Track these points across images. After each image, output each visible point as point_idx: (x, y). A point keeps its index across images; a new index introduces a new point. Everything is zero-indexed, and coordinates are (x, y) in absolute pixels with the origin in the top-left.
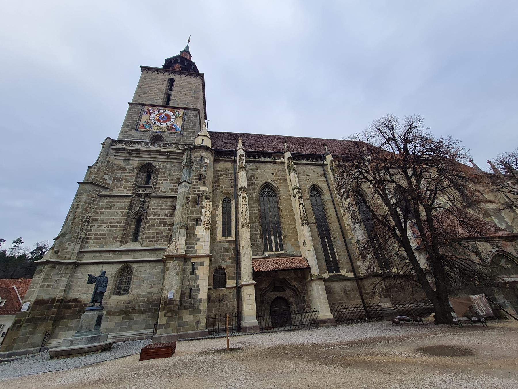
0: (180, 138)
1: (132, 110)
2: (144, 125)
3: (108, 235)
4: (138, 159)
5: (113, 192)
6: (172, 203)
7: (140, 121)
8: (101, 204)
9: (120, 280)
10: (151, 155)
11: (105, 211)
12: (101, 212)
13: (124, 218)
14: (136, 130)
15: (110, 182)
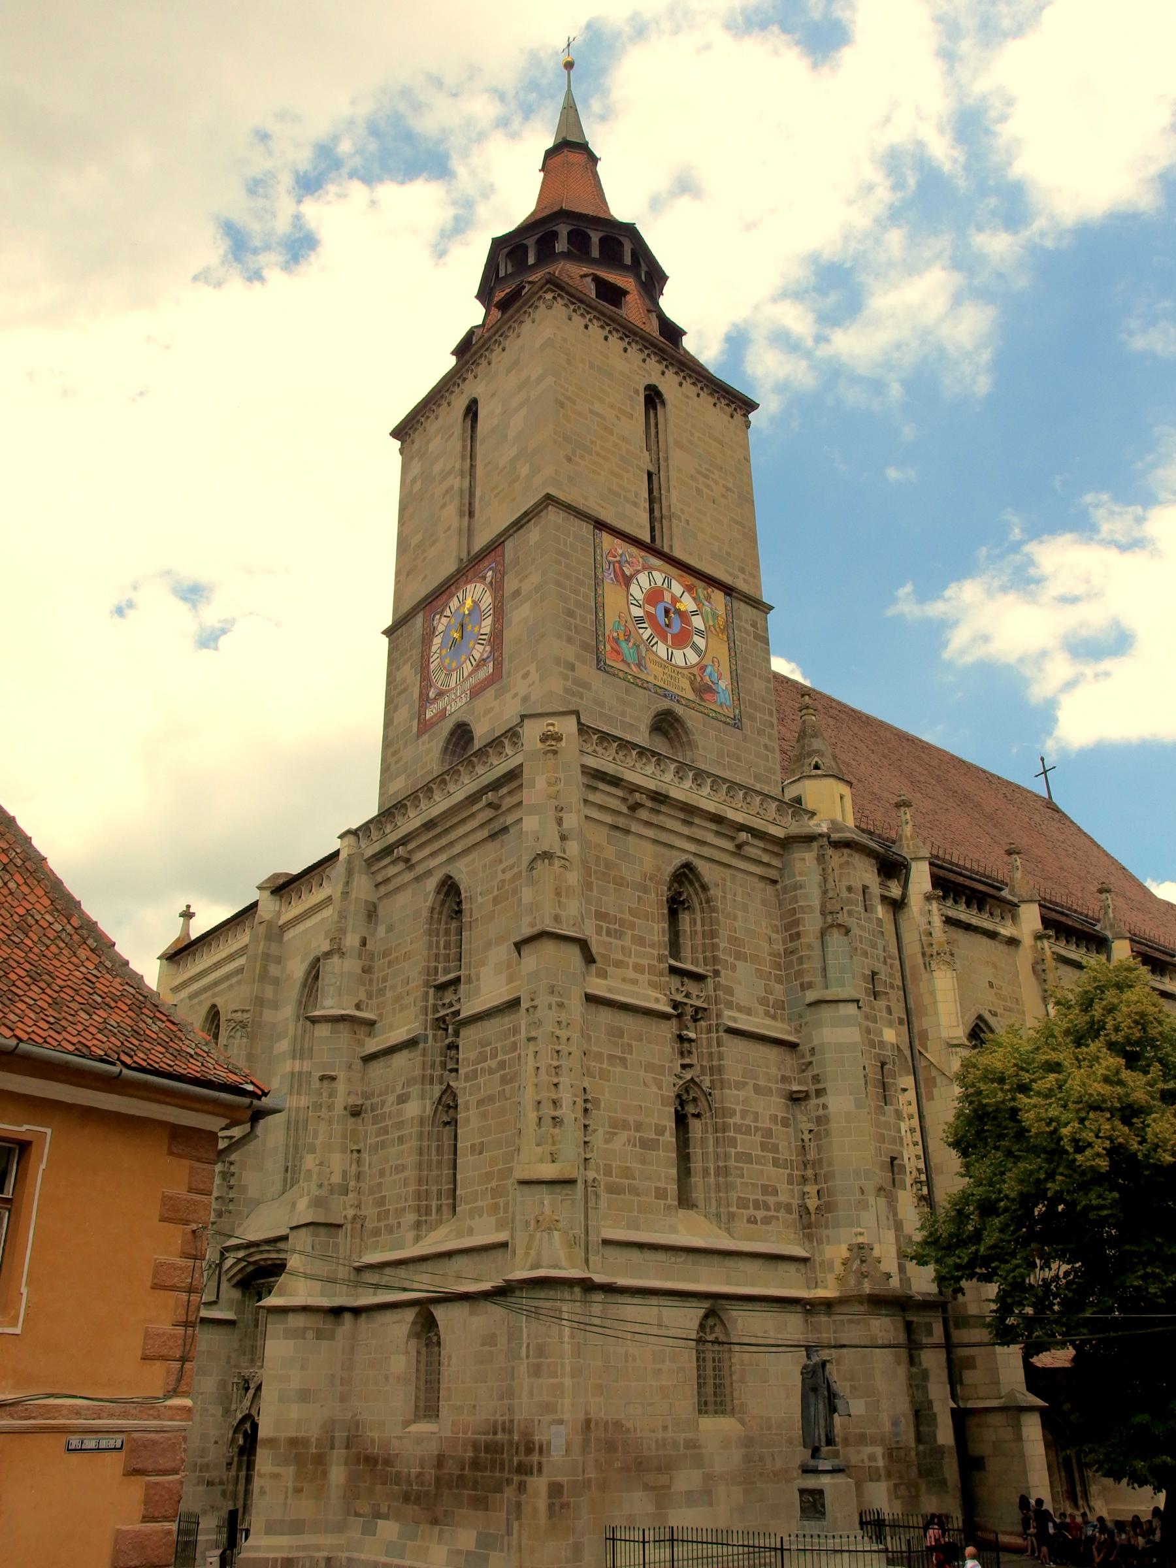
1: (565, 545)
4: (650, 833)
5: (609, 982)
6: (779, 1069)
10: (690, 824)
11: (612, 1069)
12: (604, 1075)
14: (601, 665)
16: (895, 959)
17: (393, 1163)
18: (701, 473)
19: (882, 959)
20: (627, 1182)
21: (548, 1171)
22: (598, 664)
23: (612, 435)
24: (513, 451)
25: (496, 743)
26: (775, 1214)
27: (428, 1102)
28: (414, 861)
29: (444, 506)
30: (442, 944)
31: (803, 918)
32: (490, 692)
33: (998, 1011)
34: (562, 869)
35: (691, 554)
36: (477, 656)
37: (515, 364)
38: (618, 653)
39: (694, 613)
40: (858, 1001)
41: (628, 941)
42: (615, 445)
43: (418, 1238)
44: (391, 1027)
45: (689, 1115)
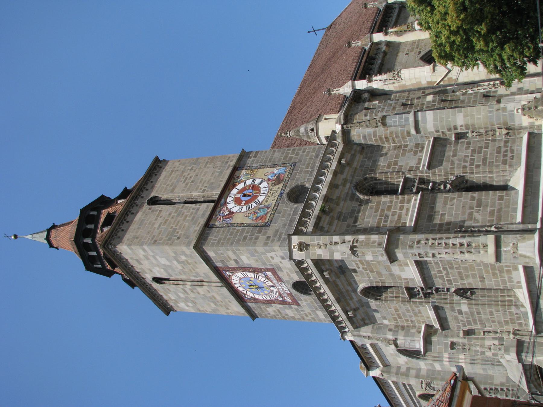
1: (215, 240)
2: (257, 218)
3: (495, 207)
8: (431, 228)
13: (465, 194)
16: (396, 95)
17: (489, 317)
18: (185, 181)
19: (396, 101)
20: (496, 213)
21: (491, 248)
22: (267, 226)
23: (168, 219)
24: (175, 262)
25: (304, 271)
26: (509, 147)
27: (462, 301)
28: (354, 307)
29: (198, 293)
30: (391, 295)
31: (379, 136)
32: (280, 273)
33: (418, 51)
34: (358, 242)
35: (220, 185)
36: (264, 279)
37: (138, 261)
39: (245, 184)
40: (415, 112)
41: (390, 213)
42: (173, 218)
43: (523, 306)
44: (429, 317)
45: (467, 185)
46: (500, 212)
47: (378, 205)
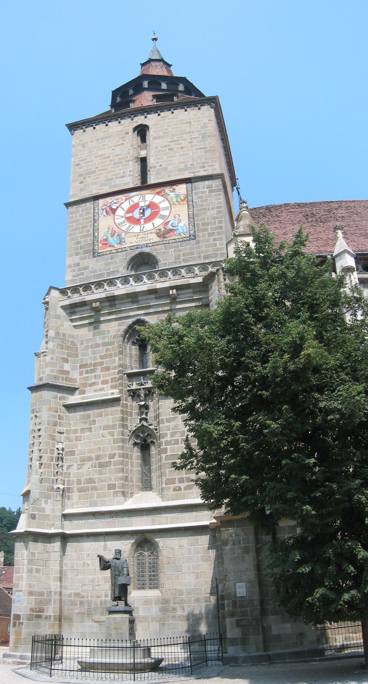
0: (192, 248)
2: (106, 240)
3: (98, 483)
4: (114, 317)
7: (96, 234)
9: (139, 564)
14: (95, 254)
15: (75, 375)
22: (93, 255)
35: (162, 178)
38: (106, 244)
46: (91, 490)
47: (111, 356)
